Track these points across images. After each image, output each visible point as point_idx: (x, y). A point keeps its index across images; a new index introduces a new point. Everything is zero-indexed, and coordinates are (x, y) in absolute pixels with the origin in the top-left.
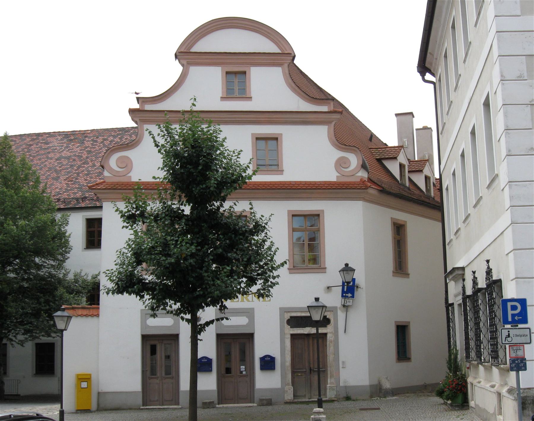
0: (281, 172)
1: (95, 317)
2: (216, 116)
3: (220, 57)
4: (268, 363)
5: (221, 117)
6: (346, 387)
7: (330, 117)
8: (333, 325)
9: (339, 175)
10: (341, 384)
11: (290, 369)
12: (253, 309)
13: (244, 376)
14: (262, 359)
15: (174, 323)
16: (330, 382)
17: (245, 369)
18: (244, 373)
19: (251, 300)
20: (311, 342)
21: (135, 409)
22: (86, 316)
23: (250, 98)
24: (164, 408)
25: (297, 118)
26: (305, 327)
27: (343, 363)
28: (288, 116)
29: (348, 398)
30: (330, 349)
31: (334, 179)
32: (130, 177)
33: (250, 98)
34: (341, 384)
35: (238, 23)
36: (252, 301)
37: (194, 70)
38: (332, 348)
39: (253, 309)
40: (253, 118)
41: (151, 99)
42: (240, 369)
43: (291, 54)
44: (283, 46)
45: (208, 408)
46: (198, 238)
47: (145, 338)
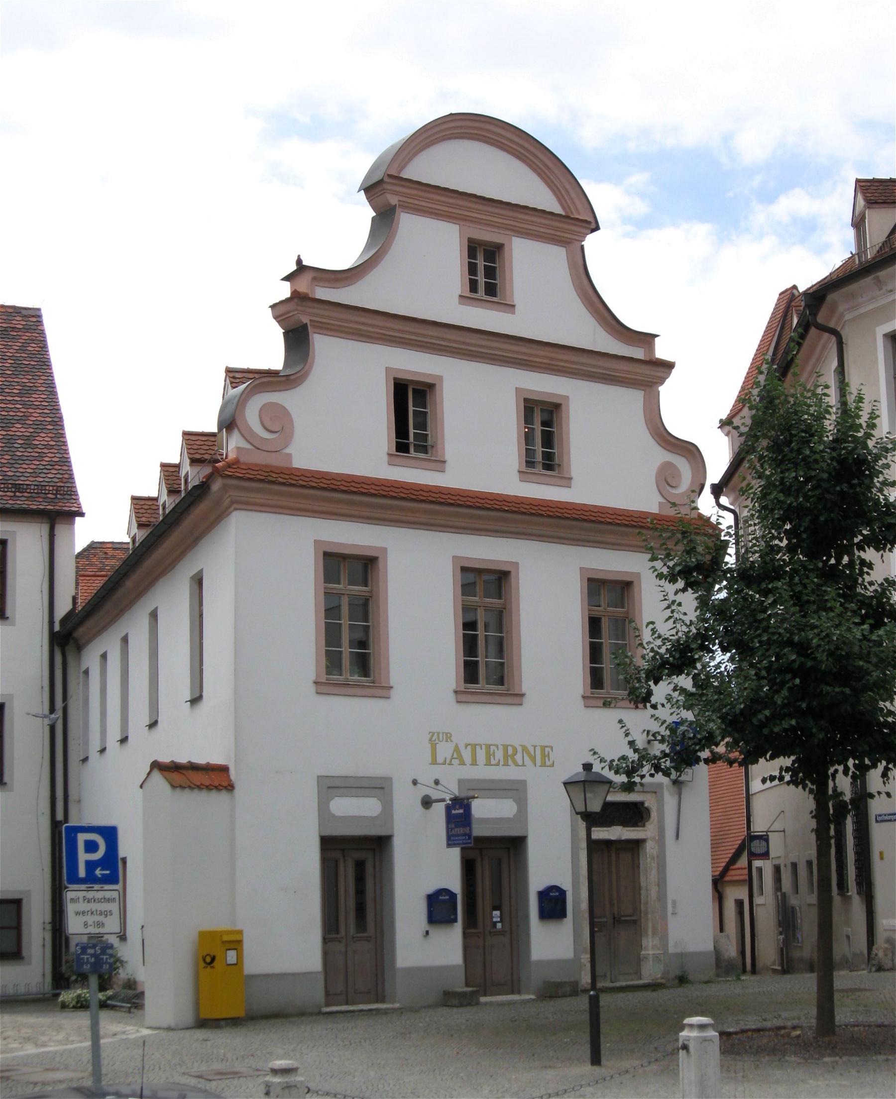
0: (567, 481)
1: (224, 792)
2: (458, 338)
3: (461, 202)
4: (553, 904)
5: (468, 341)
6: (681, 955)
7: (652, 373)
8: (655, 822)
9: (663, 500)
10: (671, 950)
11: (586, 915)
12: (523, 783)
13: (501, 933)
14: (543, 895)
15: (334, 815)
16: (650, 945)
17: (501, 917)
18: (499, 926)
19: (520, 763)
20: (613, 857)
21: (311, 1014)
22: (209, 788)
23: (510, 307)
24: (371, 1010)
25: (594, 366)
26: (610, 826)
27: (674, 903)
28: (584, 359)
29: (682, 980)
30: (649, 878)
31: (655, 510)
32: (290, 455)
33: (510, 307)
34: (671, 950)
35: (489, 131)
36: (523, 765)
37: (409, 224)
38: (654, 872)
39: (523, 783)
40: (524, 354)
41: (332, 276)
42: (492, 917)
43: (590, 223)
44: (574, 203)
45: (470, 1004)
46: (760, 635)
47: (328, 843)
